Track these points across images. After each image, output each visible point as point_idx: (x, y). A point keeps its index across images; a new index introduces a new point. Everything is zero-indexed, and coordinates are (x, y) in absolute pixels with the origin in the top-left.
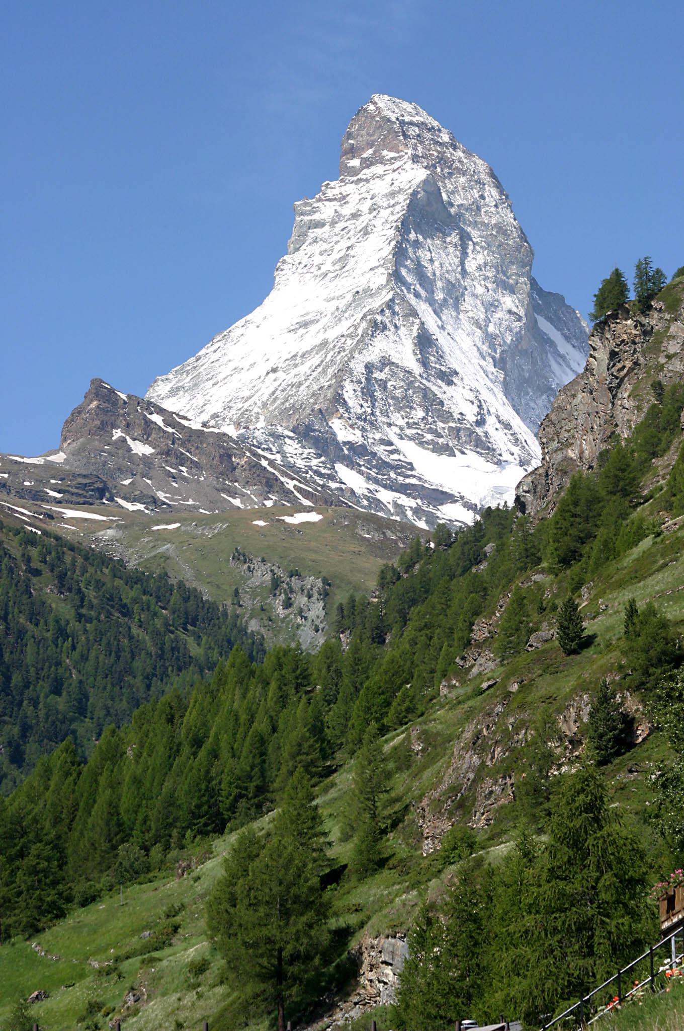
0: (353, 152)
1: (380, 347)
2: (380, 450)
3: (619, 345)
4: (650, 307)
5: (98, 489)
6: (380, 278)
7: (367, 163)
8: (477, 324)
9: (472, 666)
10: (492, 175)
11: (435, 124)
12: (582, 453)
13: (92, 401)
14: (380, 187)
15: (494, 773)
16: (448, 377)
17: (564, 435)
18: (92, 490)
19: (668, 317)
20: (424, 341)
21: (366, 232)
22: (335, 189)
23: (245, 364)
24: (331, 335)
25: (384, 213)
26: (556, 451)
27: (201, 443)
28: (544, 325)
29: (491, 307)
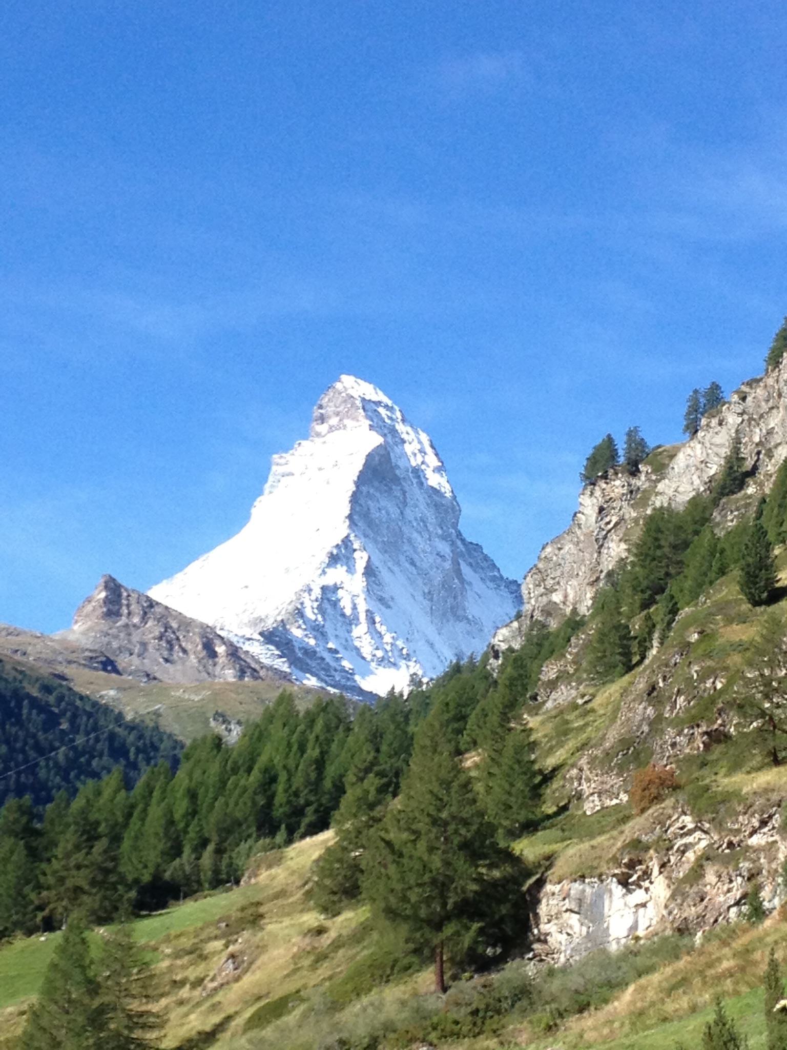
0: (322, 419)
3: (607, 502)
4: (638, 470)
5: (102, 662)
7: (331, 429)
9: (544, 702)
10: (432, 446)
12: (566, 596)
13: (101, 591)
15: (678, 724)
17: (550, 582)
18: (97, 662)
19: (654, 478)
26: (541, 596)
27: (188, 632)
28: (465, 569)
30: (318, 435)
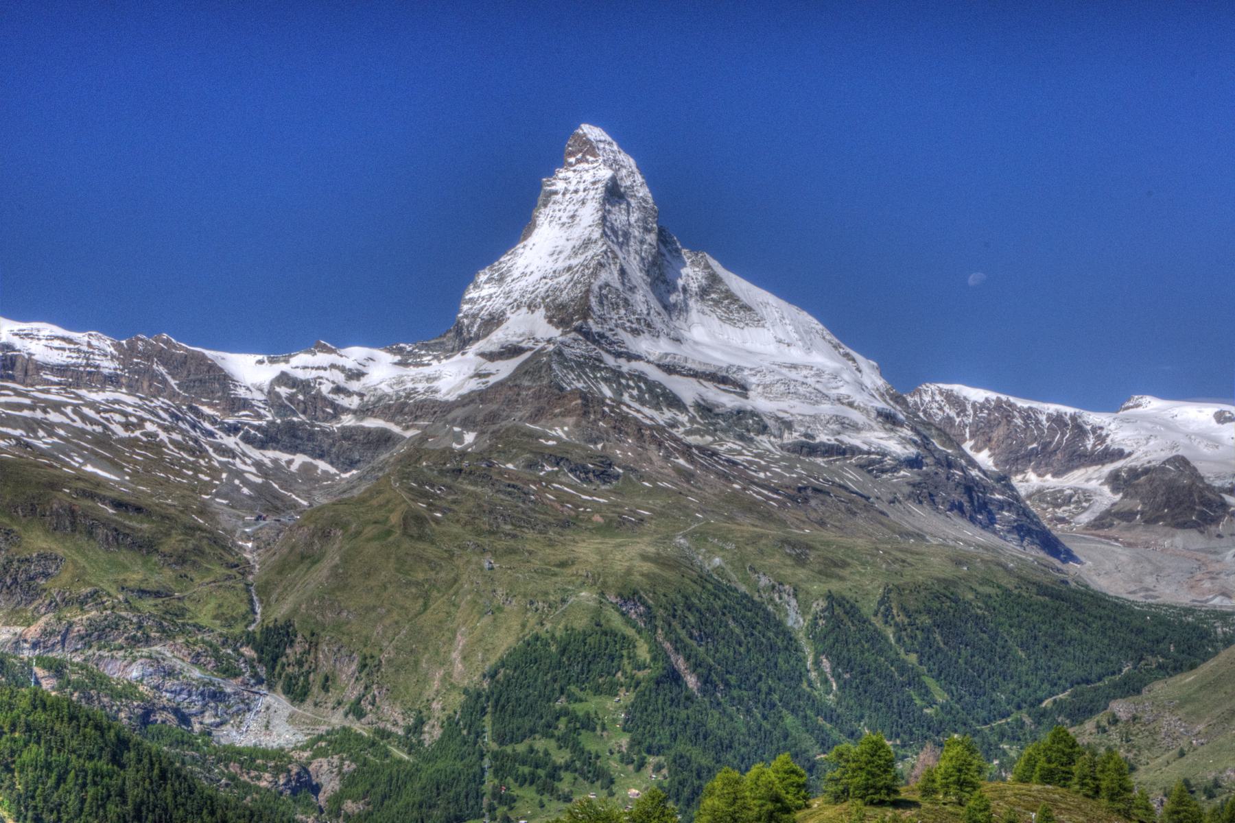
0: (572, 154)
1: (604, 276)
2: (609, 334)
6: (596, 234)
7: (578, 161)
8: (636, 252)
11: (609, 139)
14: (588, 177)
16: (632, 289)
20: (623, 272)
21: (583, 203)
22: (562, 173)
23: (528, 271)
24: (574, 262)
25: (592, 193)
29: (642, 242)
30: (571, 165)
